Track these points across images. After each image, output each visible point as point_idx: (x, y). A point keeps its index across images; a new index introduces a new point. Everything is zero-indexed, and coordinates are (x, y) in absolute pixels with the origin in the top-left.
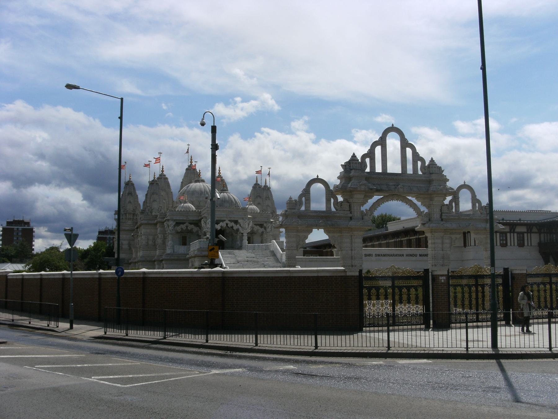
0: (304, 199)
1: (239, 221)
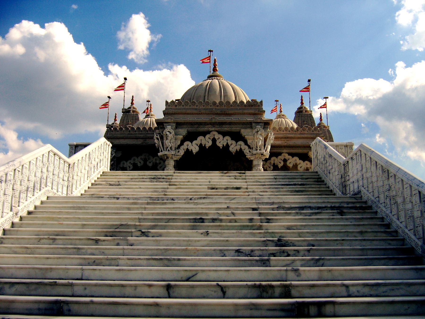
1: (245, 132)
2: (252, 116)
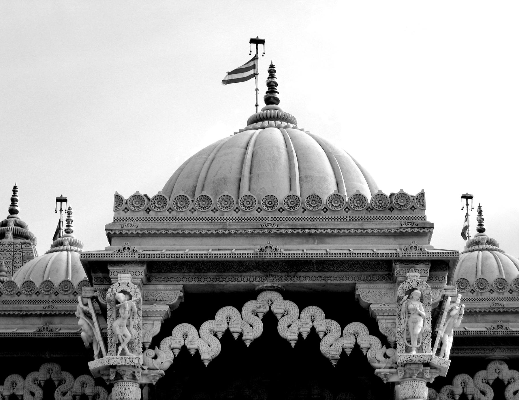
1: (369, 293)
2: (391, 240)
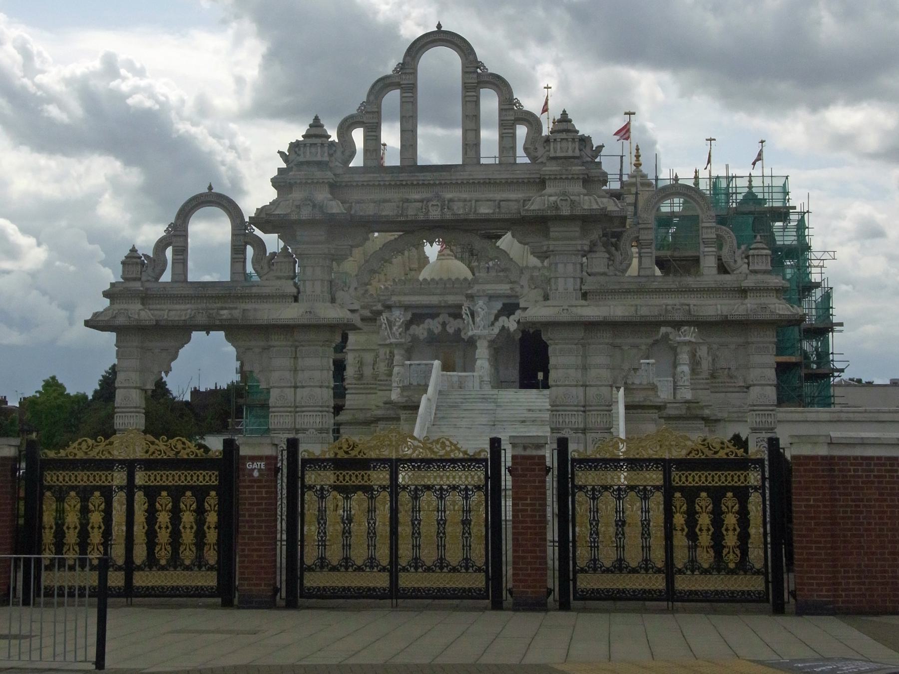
0: (169, 252)
